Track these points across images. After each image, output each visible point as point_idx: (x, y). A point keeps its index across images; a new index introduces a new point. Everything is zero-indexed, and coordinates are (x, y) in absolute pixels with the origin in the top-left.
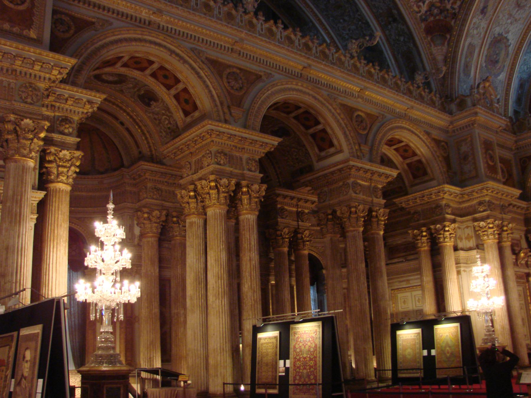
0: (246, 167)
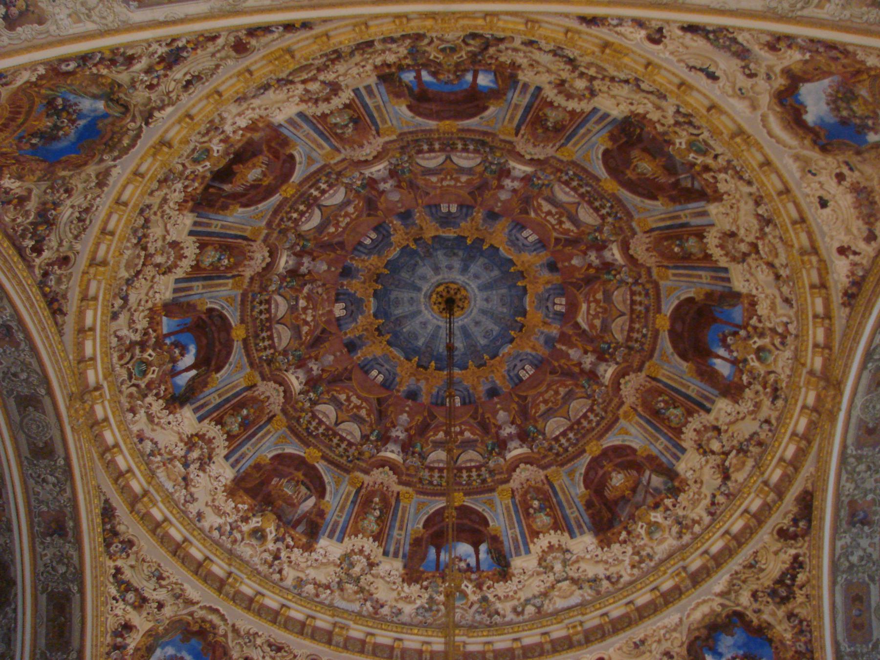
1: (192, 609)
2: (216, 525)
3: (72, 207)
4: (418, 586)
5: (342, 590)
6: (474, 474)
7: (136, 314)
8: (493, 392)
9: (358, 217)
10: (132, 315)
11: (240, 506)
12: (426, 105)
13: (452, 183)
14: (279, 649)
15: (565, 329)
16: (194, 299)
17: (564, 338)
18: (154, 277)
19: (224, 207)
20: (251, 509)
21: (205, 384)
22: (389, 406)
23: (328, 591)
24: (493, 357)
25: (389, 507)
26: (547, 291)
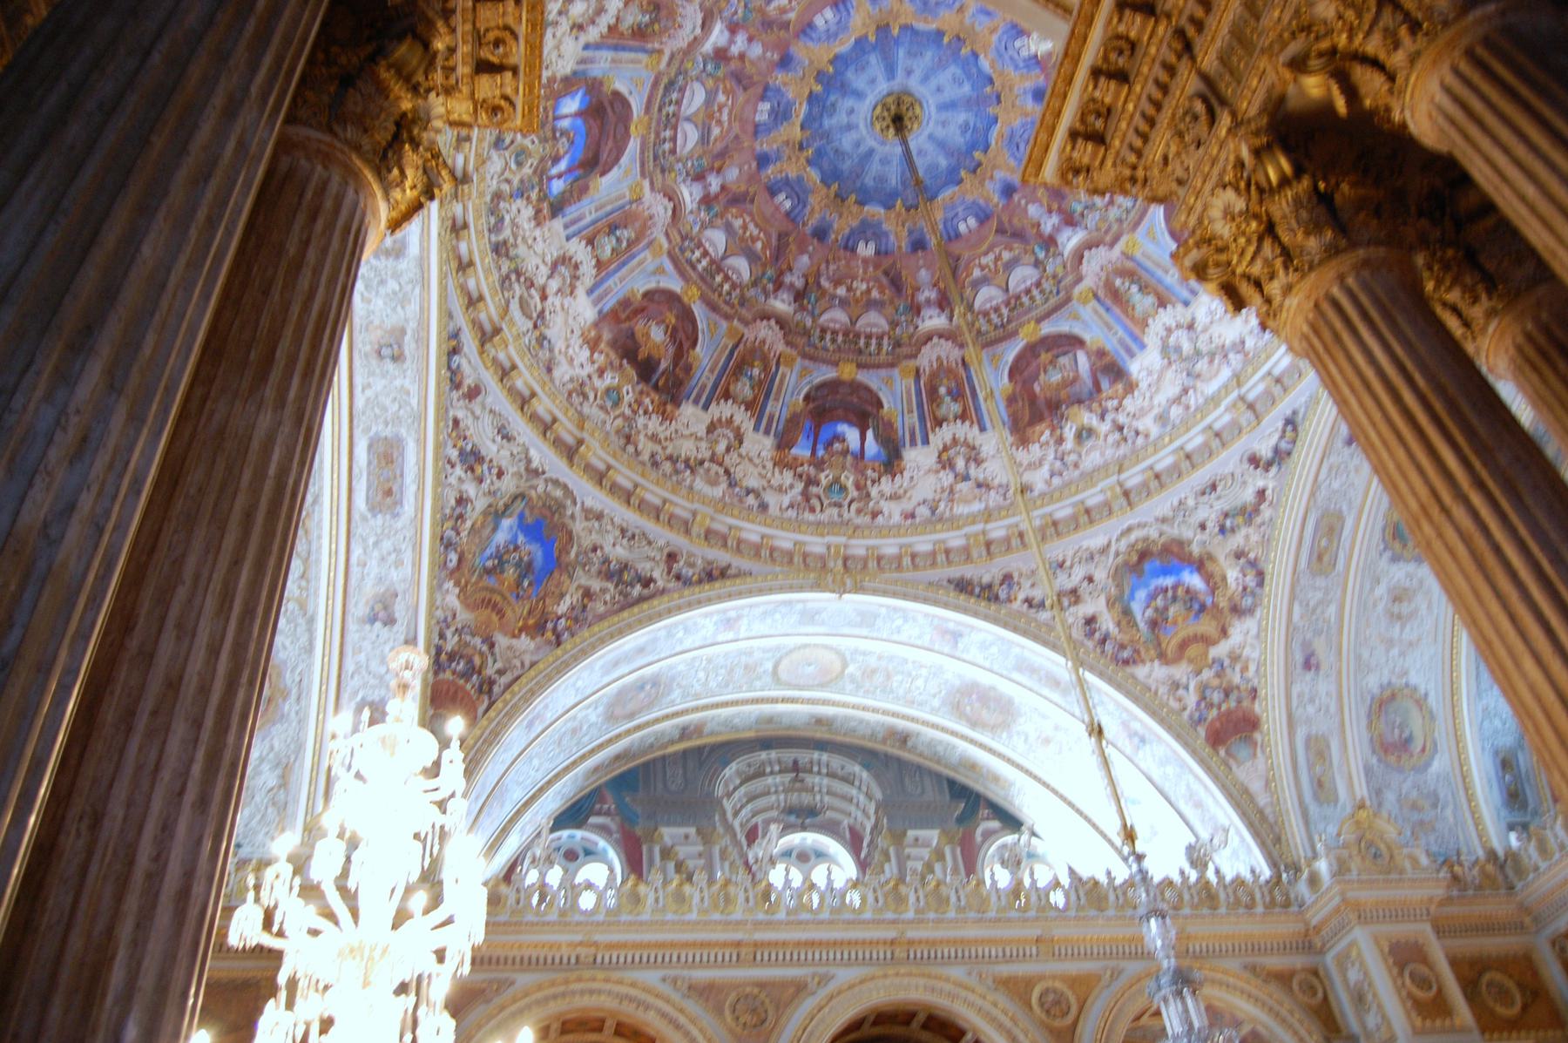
2: (1047, 476)
5: (1198, 376)
9: (751, 214)
10: (771, 487)
11: (1043, 438)
12: (604, 156)
16: (785, 415)
18: (740, 456)
19: (688, 369)
21: (889, 425)
22: (1010, 221)
23: (1191, 392)
24: (991, 81)
25: (1131, 272)
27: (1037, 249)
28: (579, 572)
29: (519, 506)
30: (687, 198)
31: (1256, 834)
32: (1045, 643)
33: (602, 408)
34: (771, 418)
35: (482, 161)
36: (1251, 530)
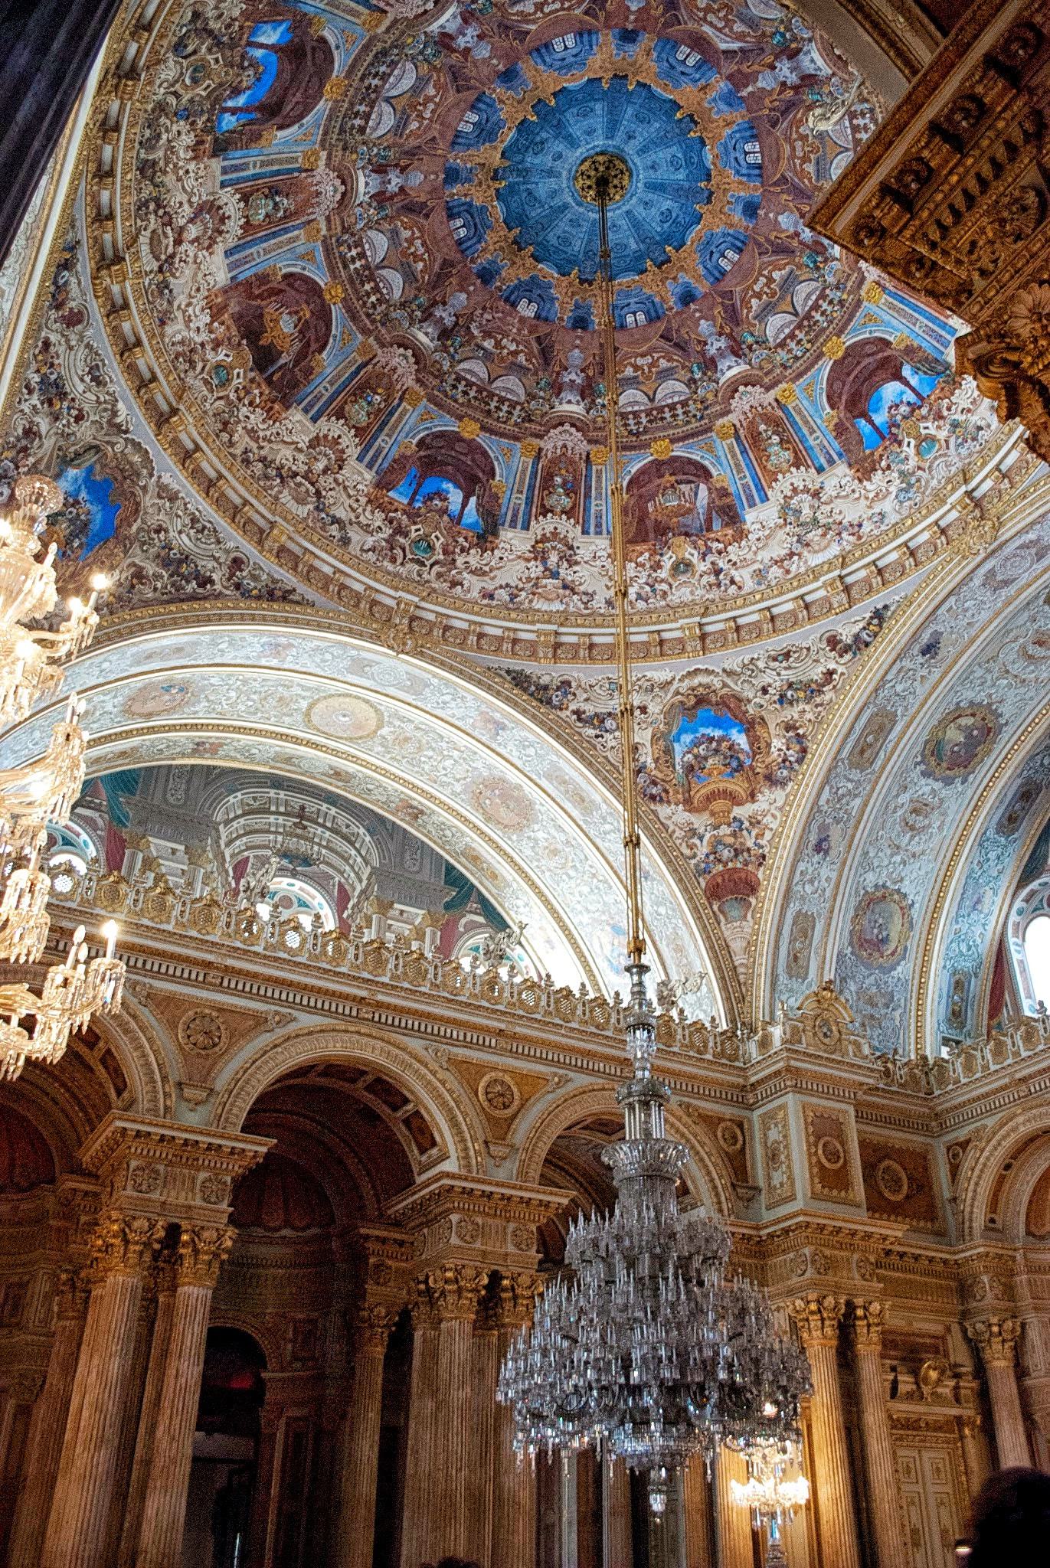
0: (199, 1195)
1: (673, 688)
3: (180, 532)
4: (880, 472)
5: (808, 545)
6: (825, 306)
7: (362, 518)
8: (751, 209)
10: (358, 523)
11: (640, 559)
13: (431, 106)
14: (787, 655)
15: (726, 71)
16: (395, 453)
17: (739, 80)
18: (336, 480)
19: (309, 371)
20: (653, 553)
22: (678, 331)
23: (796, 558)
24: (708, 177)
25: (779, 421)
26: (659, 59)
27: (695, 369)
28: (136, 549)
29: (91, 459)
30: (362, 188)
31: (724, 988)
32: (582, 758)
33: (206, 382)
34: (379, 451)
35: (157, 61)
36: (807, 708)
